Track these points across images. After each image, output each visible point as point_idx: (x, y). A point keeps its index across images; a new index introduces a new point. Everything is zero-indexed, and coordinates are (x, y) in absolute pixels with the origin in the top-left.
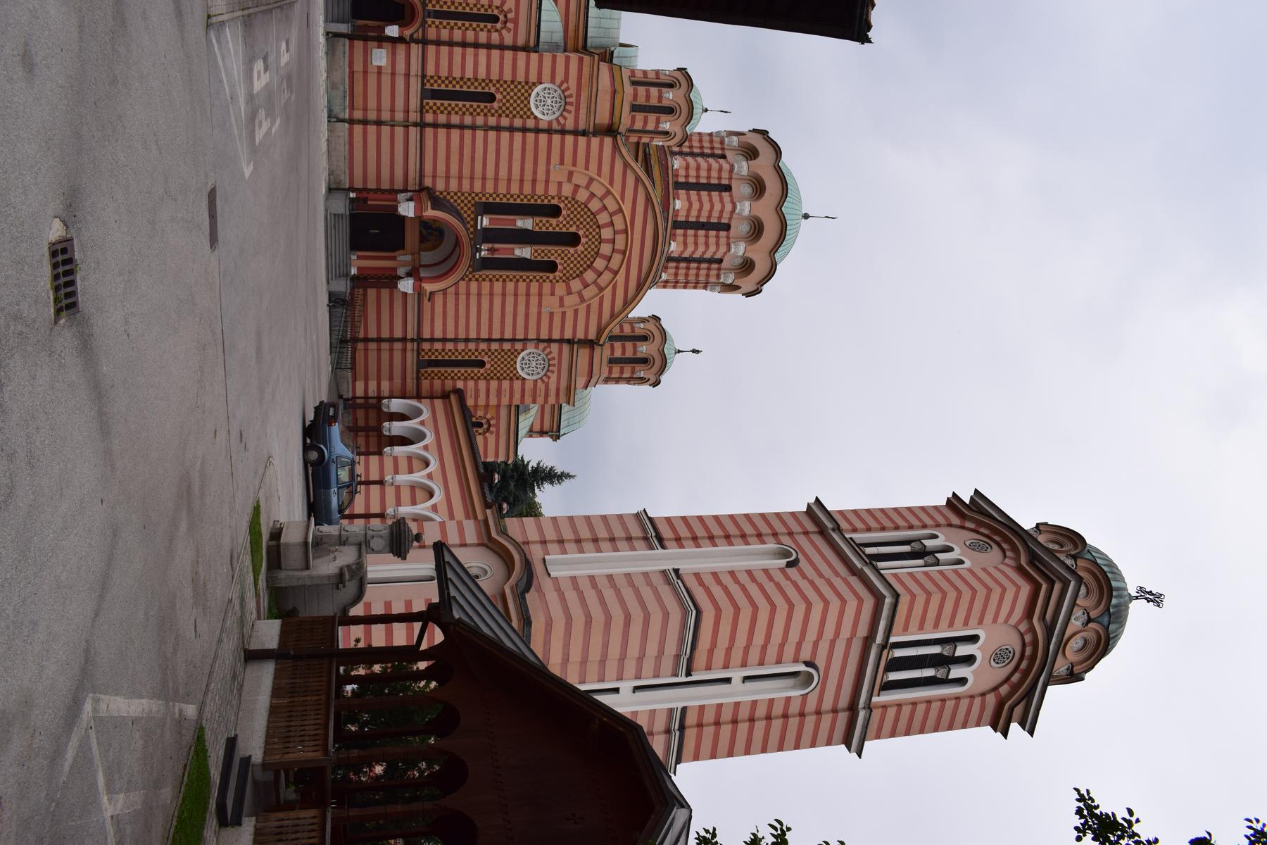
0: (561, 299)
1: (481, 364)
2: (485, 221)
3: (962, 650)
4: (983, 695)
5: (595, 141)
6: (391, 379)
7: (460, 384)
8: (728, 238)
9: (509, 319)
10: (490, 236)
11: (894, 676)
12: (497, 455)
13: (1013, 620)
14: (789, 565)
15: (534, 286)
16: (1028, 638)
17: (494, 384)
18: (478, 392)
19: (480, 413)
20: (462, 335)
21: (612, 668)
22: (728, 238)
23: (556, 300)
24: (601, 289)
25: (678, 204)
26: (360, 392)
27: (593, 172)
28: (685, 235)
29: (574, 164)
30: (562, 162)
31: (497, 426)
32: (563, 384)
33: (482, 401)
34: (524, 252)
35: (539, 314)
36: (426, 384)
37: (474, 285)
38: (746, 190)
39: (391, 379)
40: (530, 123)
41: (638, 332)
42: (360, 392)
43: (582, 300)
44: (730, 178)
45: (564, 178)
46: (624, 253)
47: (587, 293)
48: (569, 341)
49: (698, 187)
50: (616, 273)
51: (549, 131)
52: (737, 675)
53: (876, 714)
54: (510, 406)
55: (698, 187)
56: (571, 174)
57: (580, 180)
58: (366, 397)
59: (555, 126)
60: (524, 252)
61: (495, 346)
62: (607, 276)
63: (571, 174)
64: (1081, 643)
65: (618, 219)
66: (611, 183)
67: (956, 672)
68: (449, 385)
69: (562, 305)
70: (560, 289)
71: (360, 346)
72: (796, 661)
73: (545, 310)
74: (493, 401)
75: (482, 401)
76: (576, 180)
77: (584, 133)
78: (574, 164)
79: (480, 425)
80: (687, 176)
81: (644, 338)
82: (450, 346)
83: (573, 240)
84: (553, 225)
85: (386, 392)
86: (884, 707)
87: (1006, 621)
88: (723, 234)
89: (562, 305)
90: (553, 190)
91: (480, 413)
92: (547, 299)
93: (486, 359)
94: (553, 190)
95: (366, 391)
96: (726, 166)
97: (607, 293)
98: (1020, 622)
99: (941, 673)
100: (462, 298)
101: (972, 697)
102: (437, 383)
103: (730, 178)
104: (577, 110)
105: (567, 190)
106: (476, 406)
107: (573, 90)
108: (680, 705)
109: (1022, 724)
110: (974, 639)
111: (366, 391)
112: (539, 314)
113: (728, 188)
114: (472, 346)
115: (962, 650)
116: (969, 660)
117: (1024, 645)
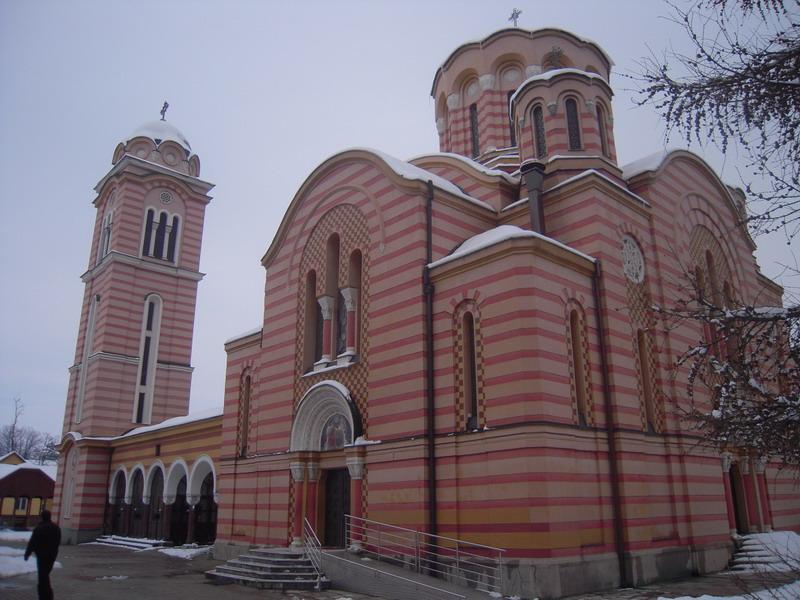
3: (157, 219)
4: (186, 207)
11: (165, 254)
13: (144, 192)
14: (98, 300)
16: (157, 184)
21: (126, 397)
52: (144, 333)
53: (184, 264)
64: (171, 156)
67: (170, 222)
72: (143, 305)
86: (181, 259)
87: (143, 195)
98: (146, 189)
99: (168, 231)
101: (187, 214)
108: (155, 364)
109: (208, 190)
110: (151, 213)
115: (157, 219)
116: (164, 217)
117: (160, 187)
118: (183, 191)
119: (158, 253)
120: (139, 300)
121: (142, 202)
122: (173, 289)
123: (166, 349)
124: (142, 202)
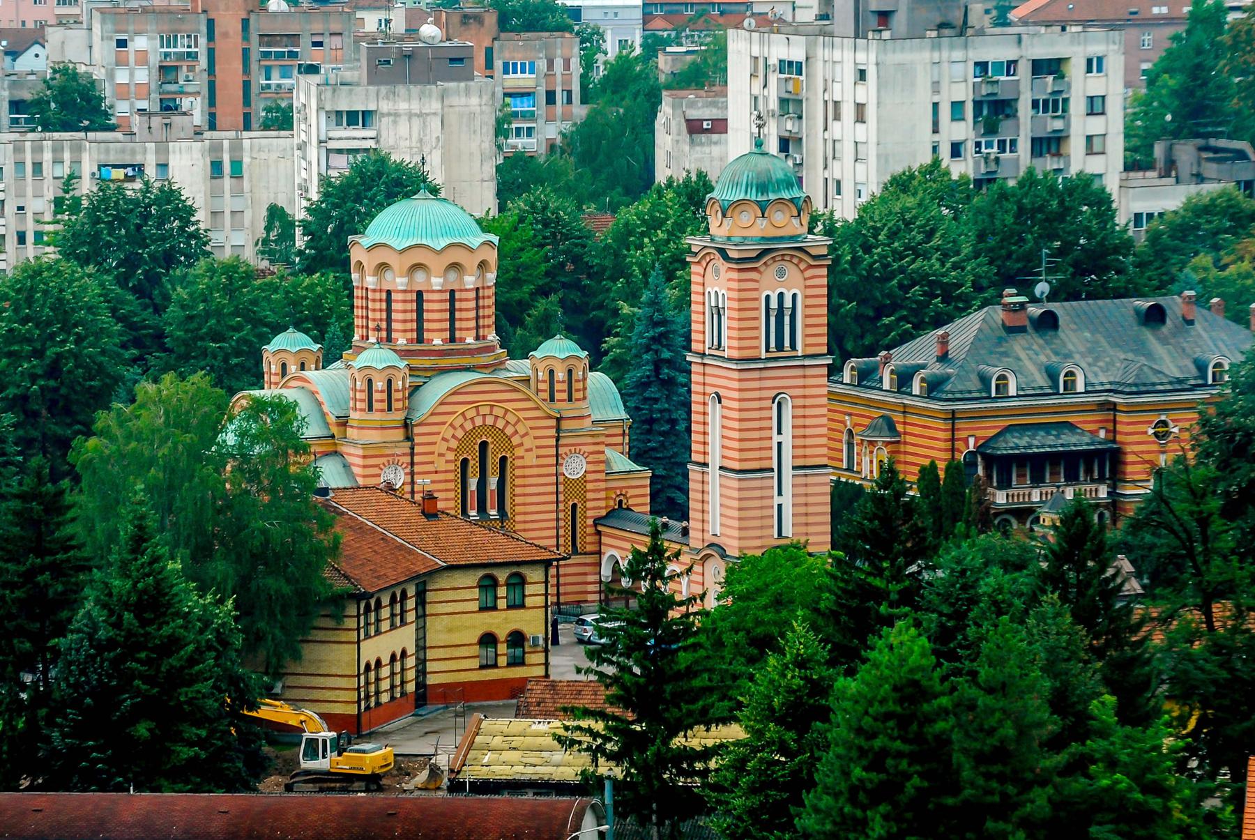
0: (527, 450)
1: (574, 506)
2: (473, 513)
5: (417, 440)
6: (585, 574)
7: (590, 522)
8: (461, 290)
9: (542, 489)
10: (482, 509)
11: (787, 343)
12: (645, 486)
15: (517, 472)
17: (590, 495)
18: (596, 506)
19: (612, 503)
20: (554, 524)
22: (461, 290)
23: (527, 455)
24: (519, 420)
25: (437, 341)
26: (596, 597)
27: (437, 438)
28: (461, 329)
29: (433, 453)
30: (432, 463)
31: (621, 488)
32: (590, 440)
33: (603, 504)
34: (493, 482)
35: (538, 466)
36: (589, 548)
37: (518, 518)
38: (420, 277)
39: (585, 574)
40: (408, 488)
41: (547, 377)
42: (596, 597)
43: (526, 434)
44: (411, 291)
45: (443, 459)
46: (492, 406)
47: (522, 432)
48: (557, 440)
49: (420, 320)
50: (507, 411)
51: (412, 474)
52: (776, 439)
54: (606, 480)
55: (420, 320)
56: (441, 455)
57: (442, 447)
58: (600, 592)
59: (408, 470)
60: (493, 482)
61: (561, 498)
62: (510, 417)
63: (441, 455)
65: (469, 415)
66: (444, 423)
68: (590, 530)
69: (531, 450)
70: (519, 452)
71: (562, 599)
72: (771, 408)
73: (535, 462)
74: (603, 495)
75: (603, 504)
76: (443, 450)
77: (412, 448)
78: (433, 453)
79: (621, 502)
80: (412, 330)
81: (551, 372)
82: (562, 532)
83: (484, 446)
84: (474, 465)
85: (596, 578)
87: (756, 281)
88: (457, 295)
89: (531, 450)
90: (451, 467)
91: (612, 503)
92: (527, 462)
93: (571, 503)
94: (451, 467)
95: (595, 592)
96: (400, 297)
97: (521, 415)
100: (528, 526)
102: (589, 539)
103: (411, 291)
104: (393, 455)
105: (451, 456)
106: (607, 507)
107: (384, 460)
108: (791, 472)
111: (595, 592)
112: (538, 466)
113: (420, 294)
114: (561, 515)
118: (801, 260)
119: (780, 347)
120: (768, 403)
121: (756, 290)
122: (800, 382)
123: (800, 452)
124: (756, 290)
